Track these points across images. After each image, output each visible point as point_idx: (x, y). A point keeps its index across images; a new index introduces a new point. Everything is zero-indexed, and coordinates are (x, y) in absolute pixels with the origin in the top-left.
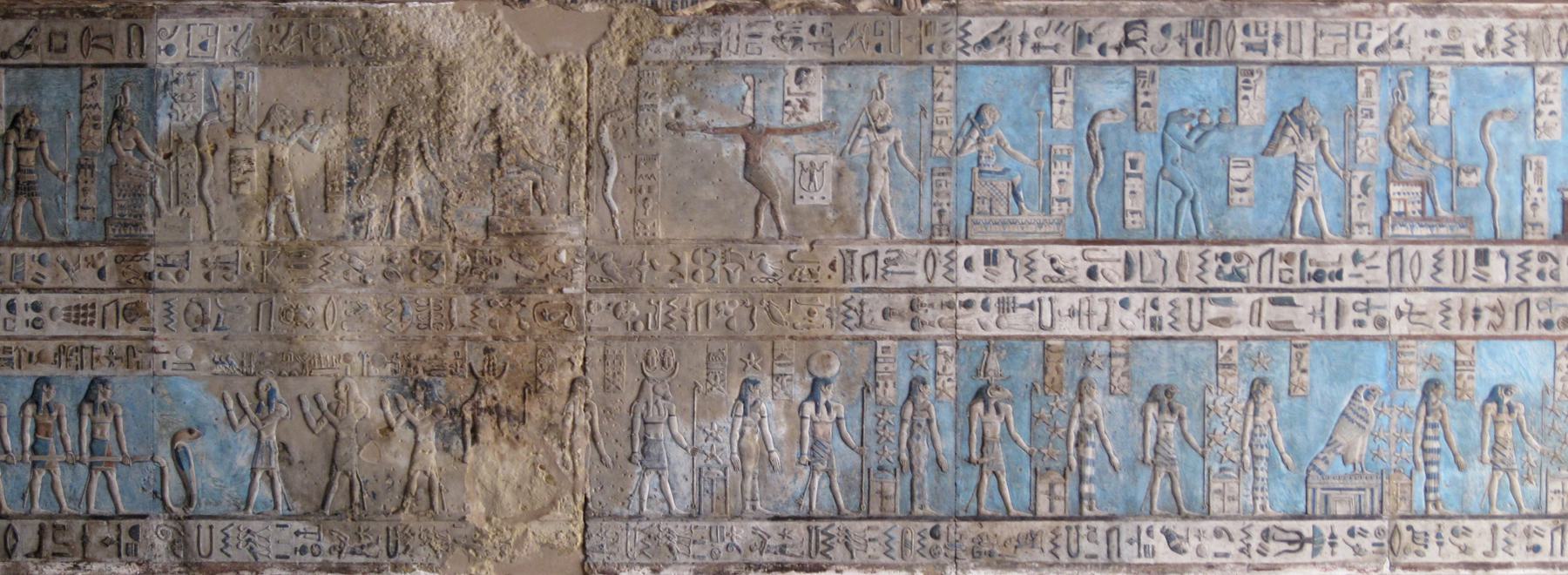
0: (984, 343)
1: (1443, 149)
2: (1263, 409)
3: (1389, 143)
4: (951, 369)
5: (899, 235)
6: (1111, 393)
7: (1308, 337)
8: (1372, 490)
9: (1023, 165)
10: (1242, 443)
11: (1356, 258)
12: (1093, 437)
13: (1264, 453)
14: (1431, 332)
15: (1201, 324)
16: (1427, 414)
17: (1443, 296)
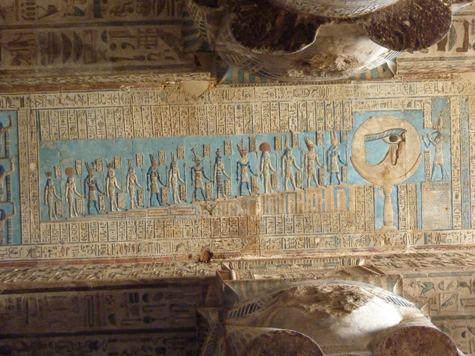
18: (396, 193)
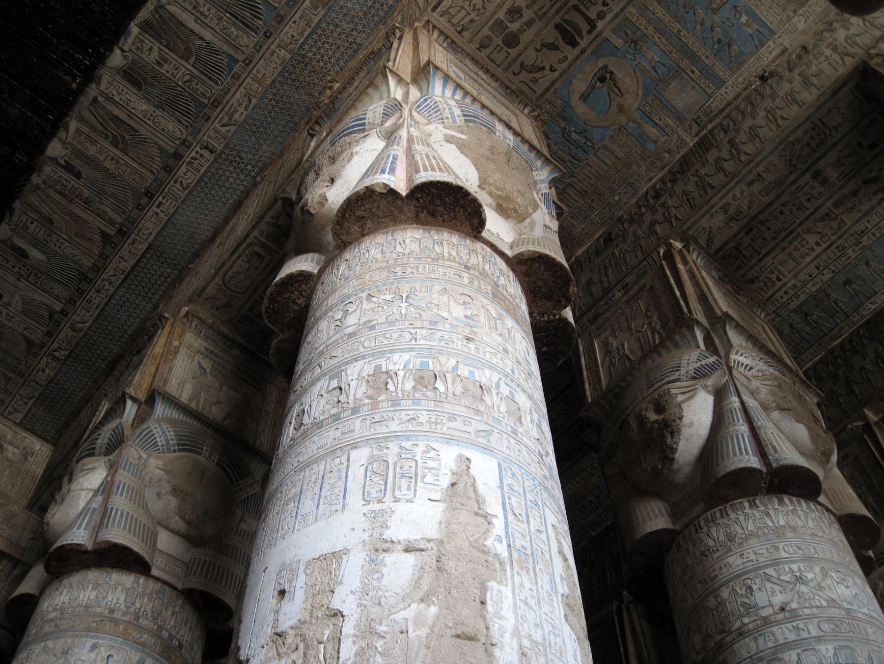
4: (795, 316)
18: (643, 114)
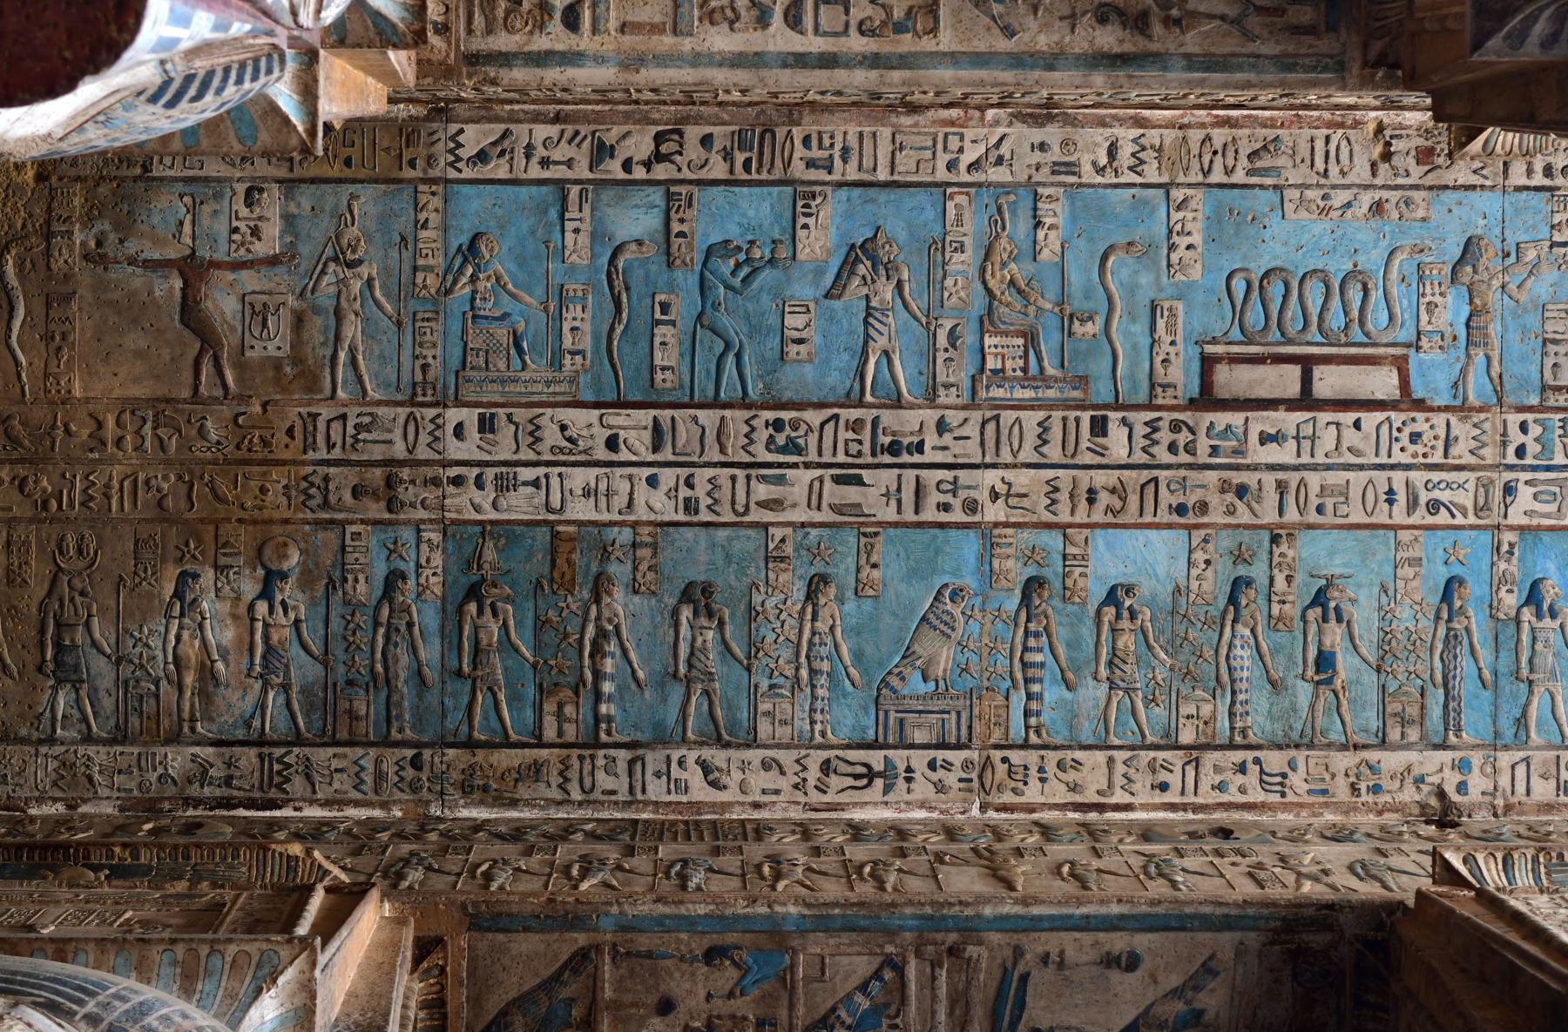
0: (478, 529)
1: (1052, 292)
2: (824, 613)
3: (984, 283)
4: (437, 560)
5: (373, 394)
6: (636, 592)
7: (880, 524)
8: (958, 713)
9: (527, 310)
10: (798, 655)
11: (942, 427)
12: (612, 646)
13: (825, 666)
14: (1034, 519)
15: (747, 507)
16: (1028, 620)
17: (1050, 474)
